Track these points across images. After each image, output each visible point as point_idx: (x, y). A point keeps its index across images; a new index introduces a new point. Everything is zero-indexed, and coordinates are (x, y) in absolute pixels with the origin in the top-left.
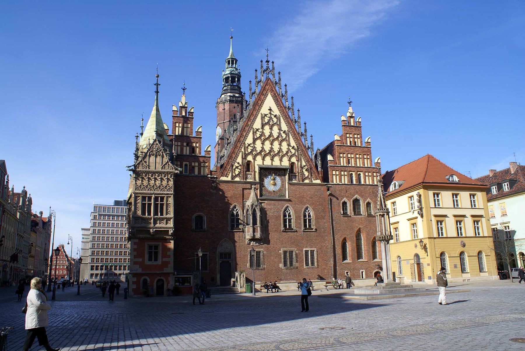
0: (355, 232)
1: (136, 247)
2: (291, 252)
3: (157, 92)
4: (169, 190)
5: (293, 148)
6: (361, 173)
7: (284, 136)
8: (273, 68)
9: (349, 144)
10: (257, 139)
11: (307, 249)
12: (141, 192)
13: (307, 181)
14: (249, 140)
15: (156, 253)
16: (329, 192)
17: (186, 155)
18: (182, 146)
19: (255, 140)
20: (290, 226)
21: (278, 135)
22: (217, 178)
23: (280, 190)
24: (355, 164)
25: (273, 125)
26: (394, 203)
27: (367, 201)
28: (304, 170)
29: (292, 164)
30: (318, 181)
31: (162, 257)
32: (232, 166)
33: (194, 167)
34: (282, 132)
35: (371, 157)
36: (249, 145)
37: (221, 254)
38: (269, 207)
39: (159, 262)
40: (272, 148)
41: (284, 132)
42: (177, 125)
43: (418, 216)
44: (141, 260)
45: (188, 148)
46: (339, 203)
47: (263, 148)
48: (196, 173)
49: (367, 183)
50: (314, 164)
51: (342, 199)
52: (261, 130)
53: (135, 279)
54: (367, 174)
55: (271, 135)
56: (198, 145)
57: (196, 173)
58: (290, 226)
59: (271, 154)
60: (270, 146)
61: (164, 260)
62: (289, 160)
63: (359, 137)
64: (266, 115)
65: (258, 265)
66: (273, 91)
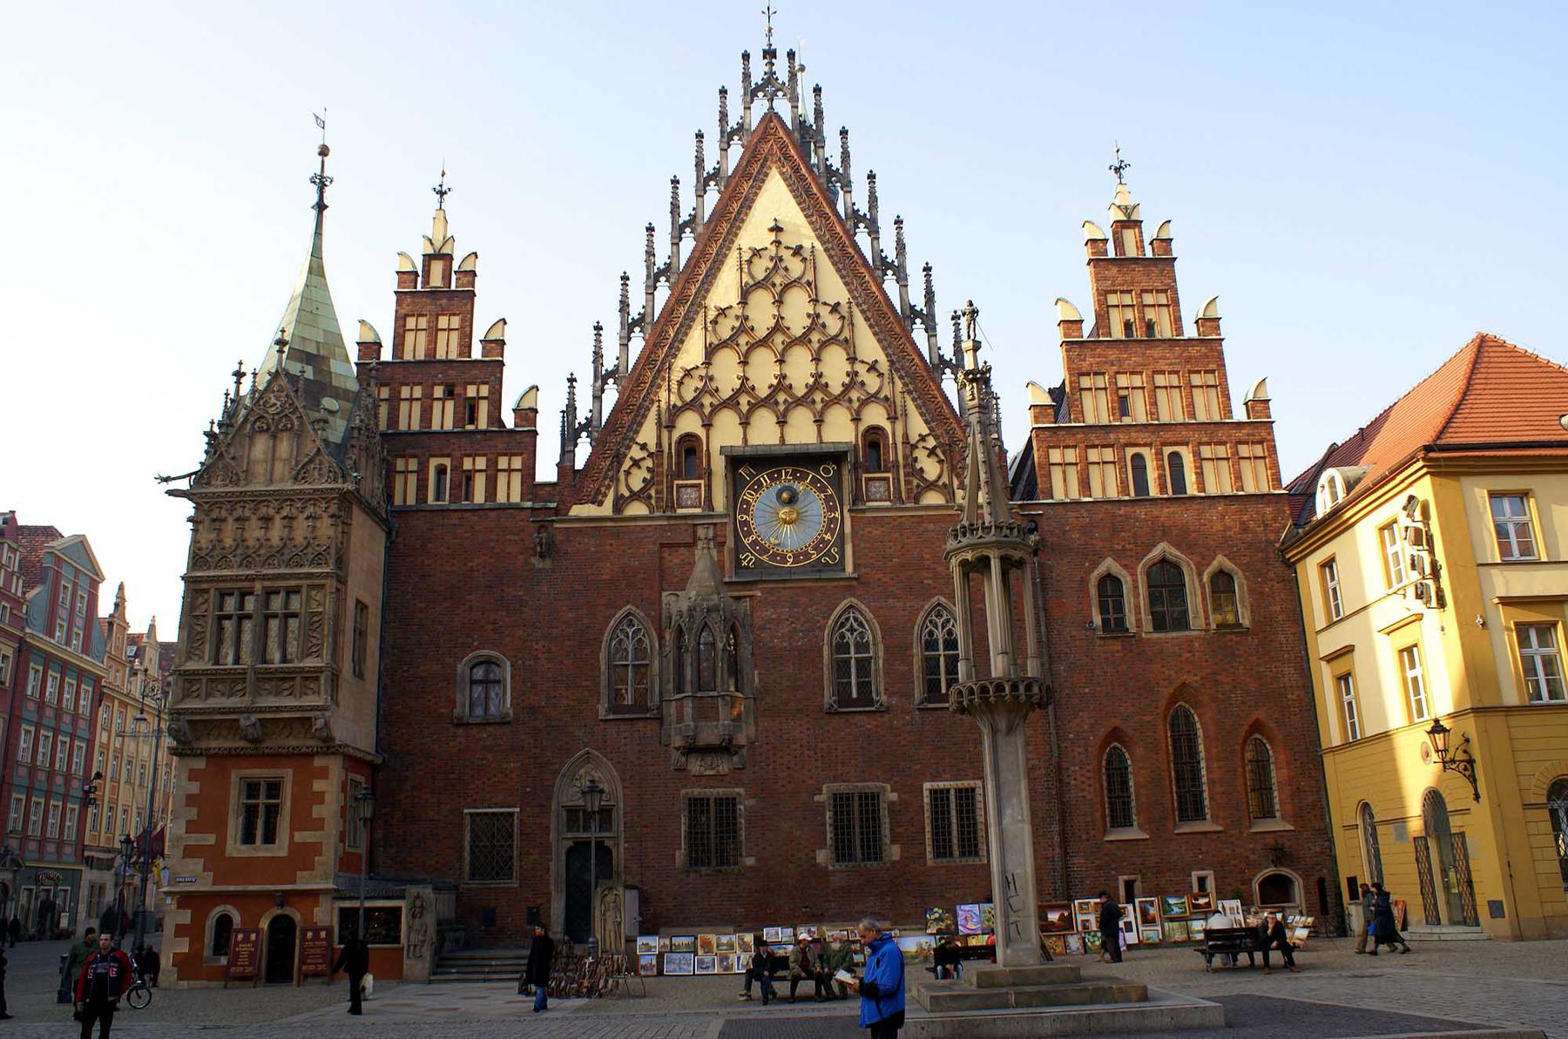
0: (1163, 703)
1: (194, 788)
2: (870, 799)
3: (321, 207)
4: (318, 559)
5: (873, 367)
7: (833, 325)
9: (1118, 333)
10: (724, 344)
11: (941, 785)
13: (933, 498)
14: (692, 353)
15: (272, 812)
18: (428, 398)
19: (711, 352)
20: (864, 687)
21: (808, 322)
22: (556, 511)
23: (820, 544)
26: (1328, 564)
27: (1215, 565)
28: (921, 454)
29: (873, 439)
31: (293, 830)
32: (618, 459)
33: (469, 477)
34: (824, 311)
35: (1224, 377)
36: (688, 373)
37: (572, 812)
38: (769, 613)
39: (280, 849)
42: (411, 323)
43: (1418, 606)
44: (211, 839)
45: (450, 405)
46: (1084, 581)
48: (479, 497)
49: (1212, 490)
51: (1095, 565)
52: (738, 311)
53: (185, 917)
56: (485, 390)
57: (479, 497)
58: (864, 687)
59: (780, 399)
61: (299, 837)
62: (856, 420)
64: (756, 253)
65: (726, 856)
66: (788, 157)
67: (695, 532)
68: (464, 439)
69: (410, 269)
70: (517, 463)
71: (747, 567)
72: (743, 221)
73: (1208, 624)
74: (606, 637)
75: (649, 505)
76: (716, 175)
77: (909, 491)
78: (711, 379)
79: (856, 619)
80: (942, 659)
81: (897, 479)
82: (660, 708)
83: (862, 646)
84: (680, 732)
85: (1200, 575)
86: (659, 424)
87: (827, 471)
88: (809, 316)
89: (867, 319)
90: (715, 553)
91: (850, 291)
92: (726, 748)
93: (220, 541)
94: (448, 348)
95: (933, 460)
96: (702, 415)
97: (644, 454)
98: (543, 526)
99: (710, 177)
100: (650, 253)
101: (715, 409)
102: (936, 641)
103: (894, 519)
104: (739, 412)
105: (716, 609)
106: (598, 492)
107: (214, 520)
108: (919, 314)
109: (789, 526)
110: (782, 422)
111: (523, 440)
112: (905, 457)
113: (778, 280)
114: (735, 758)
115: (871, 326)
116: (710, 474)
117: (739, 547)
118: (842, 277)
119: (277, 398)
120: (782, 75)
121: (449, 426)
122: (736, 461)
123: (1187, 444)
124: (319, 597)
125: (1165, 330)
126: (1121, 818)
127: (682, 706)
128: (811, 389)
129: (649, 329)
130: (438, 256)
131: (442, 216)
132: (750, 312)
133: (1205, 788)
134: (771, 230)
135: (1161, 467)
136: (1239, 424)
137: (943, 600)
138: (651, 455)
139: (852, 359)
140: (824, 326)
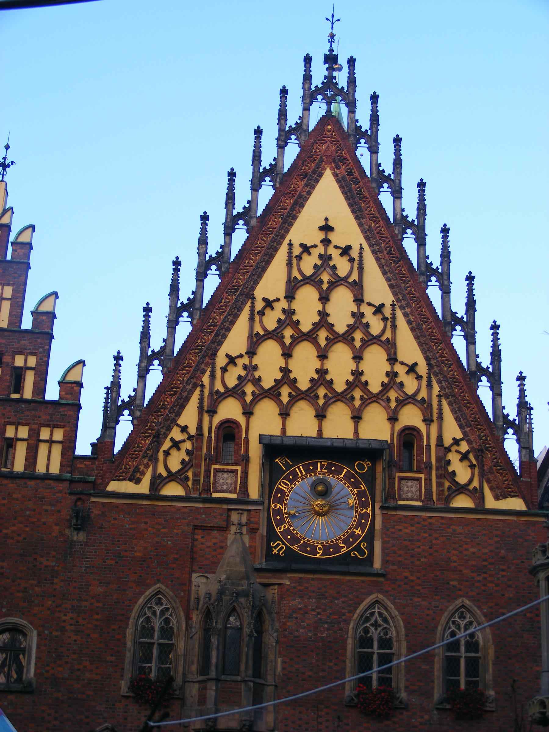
8: (352, 81)
13: (463, 502)
14: (236, 341)
21: (351, 321)
25: (333, 285)
28: (453, 457)
30: (516, 504)
32: (158, 440)
34: (368, 311)
36: (232, 360)
38: (297, 603)
40: (322, 372)
47: (285, 371)
48: (19, 466)
52: (284, 304)
56: (32, 361)
57: (19, 466)
59: (320, 394)
60: (317, 364)
62: (393, 419)
64: (306, 249)
66: (344, 161)
67: (229, 517)
70: (59, 435)
72: (295, 218)
74: (133, 614)
76: (273, 170)
77: (440, 493)
78: (255, 368)
79: (380, 614)
80: (463, 661)
82: (182, 688)
83: (385, 643)
86: (201, 408)
87: (361, 467)
88: (353, 314)
89: (409, 322)
90: (246, 539)
91: (394, 294)
95: (466, 463)
97: (185, 436)
99: (266, 172)
100: (203, 241)
101: (257, 398)
102: (457, 642)
103: (425, 519)
105: (246, 594)
106: (137, 470)
108: (459, 321)
110: (321, 416)
111: (68, 409)
112: (438, 459)
113: (325, 277)
115: (412, 330)
116: (245, 460)
117: (272, 536)
118: (388, 280)
122: (273, 449)
127: (205, 688)
128: (350, 386)
132: (295, 305)
134: (321, 228)
137: (467, 602)
138: (190, 438)
139: (392, 360)
140: (367, 325)
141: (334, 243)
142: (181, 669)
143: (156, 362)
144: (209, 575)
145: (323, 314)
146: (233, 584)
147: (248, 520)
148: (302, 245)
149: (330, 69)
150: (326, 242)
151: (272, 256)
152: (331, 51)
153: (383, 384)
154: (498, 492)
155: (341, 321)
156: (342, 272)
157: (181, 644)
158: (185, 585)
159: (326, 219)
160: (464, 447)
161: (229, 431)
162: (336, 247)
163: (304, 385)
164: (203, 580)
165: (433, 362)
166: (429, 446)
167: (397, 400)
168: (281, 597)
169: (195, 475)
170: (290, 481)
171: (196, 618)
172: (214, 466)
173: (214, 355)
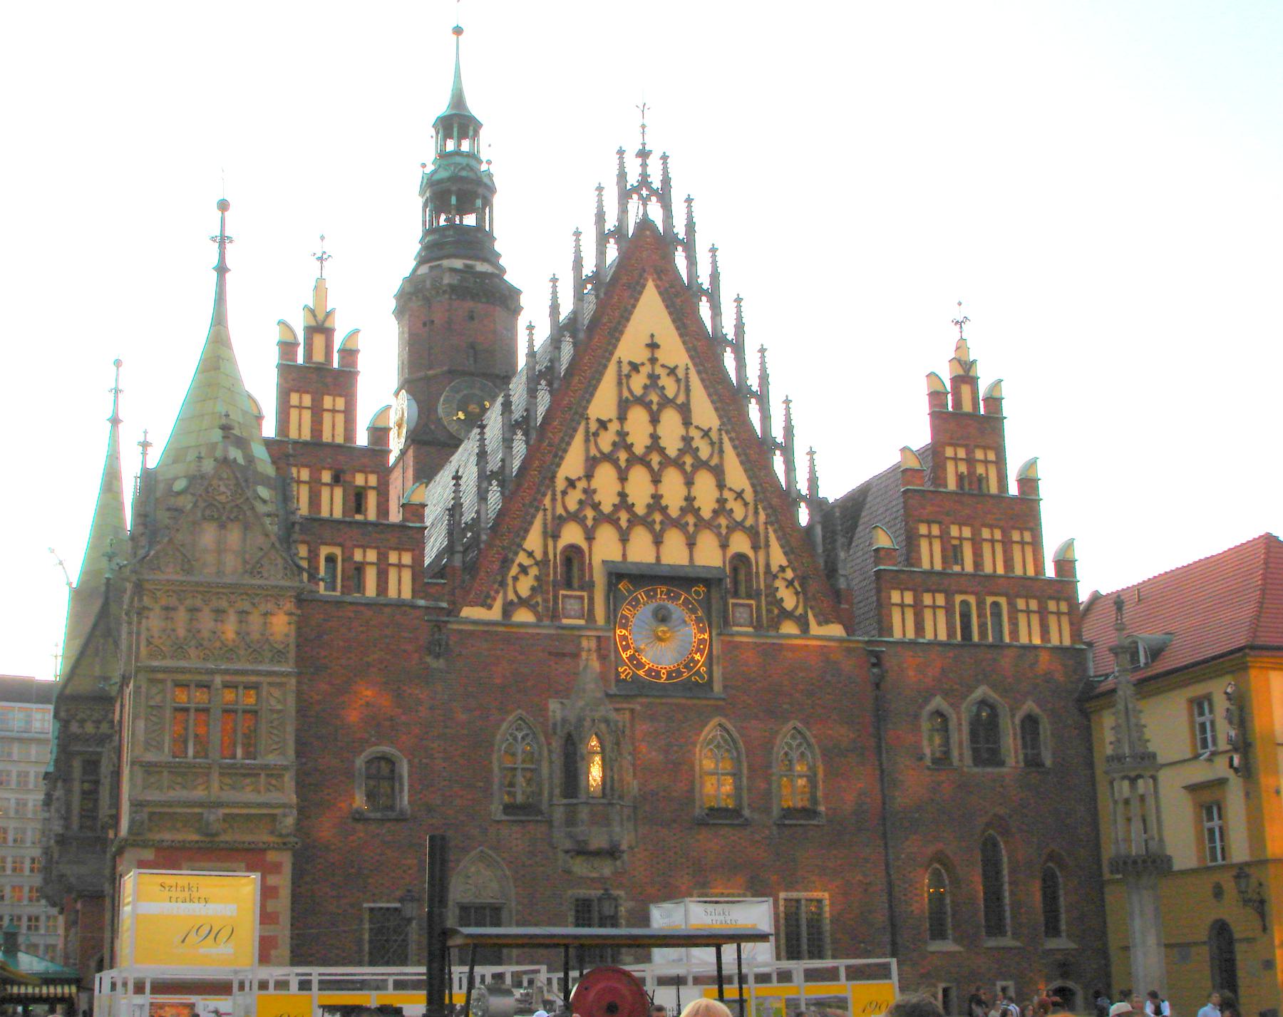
3: (222, 270)
4: (279, 655)
6: (1003, 601)
8: (666, 181)
9: (952, 485)
11: (794, 895)
12: (169, 663)
14: (572, 464)
16: (875, 670)
17: (331, 522)
19: (592, 464)
21: (681, 445)
22: (449, 613)
23: (690, 664)
24: (978, 564)
25: (662, 406)
28: (779, 583)
32: (506, 563)
33: (360, 568)
36: (571, 483)
40: (657, 497)
41: (706, 434)
42: (294, 399)
45: (338, 492)
46: (917, 717)
47: (623, 495)
48: (371, 590)
50: (821, 562)
54: (1021, 604)
55: (655, 444)
56: (373, 480)
57: (371, 590)
59: (656, 519)
60: (651, 490)
62: (724, 546)
63: (991, 456)
64: (635, 367)
67: (580, 643)
68: (353, 529)
69: (291, 340)
70: (407, 559)
71: (624, 680)
72: (622, 333)
73: (1017, 762)
75: (536, 614)
78: (595, 491)
81: (759, 607)
84: (570, 836)
85: (1013, 716)
86: (545, 534)
87: (697, 593)
89: (735, 447)
90: (596, 665)
91: (720, 417)
92: (612, 853)
93: (173, 630)
94: (332, 432)
95: (791, 589)
96: (585, 527)
98: (439, 626)
104: (619, 528)
105: (607, 721)
106: (488, 596)
107: (166, 608)
109: (664, 646)
110: (658, 542)
112: (768, 587)
113: (654, 398)
114: (618, 863)
115: (738, 455)
116: (589, 586)
118: (713, 402)
119: (227, 486)
120: (656, 183)
121: (338, 514)
123: (1006, 595)
124: (277, 693)
125: (994, 489)
126: (938, 932)
129: (534, 435)
130: (320, 328)
131: (320, 289)
132: (628, 427)
133: (1007, 908)
134: (648, 345)
135: (981, 615)
136: (1050, 581)
137: (798, 724)
139: (721, 486)
140: (697, 449)
141: (661, 361)
142: (546, 794)
143: (494, 483)
144: (565, 701)
145: (655, 437)
146: (591, 710)
147: (599, 648)
148: (630, 363)
149: (644, 165)
150: (653, 360)
151: (602, 374)
152: (644, 145)
153: (715, 511)
154: (821, 618)
155: (672, 445)
156: (670, 393)
157: (545, 771)
158: (543, 709)
159: (652, 336)
160: (789, 574)
161: (573, 556)
162: (663, 366)
163: (640, 510)
164: (559, 706)
165: (759, 488)
166: (757, 573)
167: (727, 527)
168: (632, 718)
169: (546, 601)
170: (634, 607)
171: (556, 744)
172: (562, 592)
173: (553, 477)
